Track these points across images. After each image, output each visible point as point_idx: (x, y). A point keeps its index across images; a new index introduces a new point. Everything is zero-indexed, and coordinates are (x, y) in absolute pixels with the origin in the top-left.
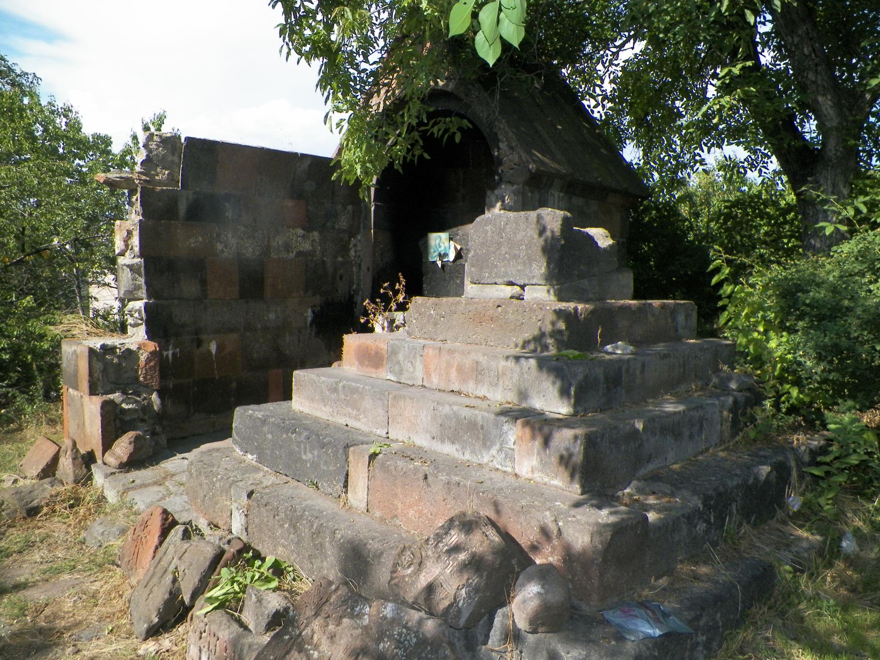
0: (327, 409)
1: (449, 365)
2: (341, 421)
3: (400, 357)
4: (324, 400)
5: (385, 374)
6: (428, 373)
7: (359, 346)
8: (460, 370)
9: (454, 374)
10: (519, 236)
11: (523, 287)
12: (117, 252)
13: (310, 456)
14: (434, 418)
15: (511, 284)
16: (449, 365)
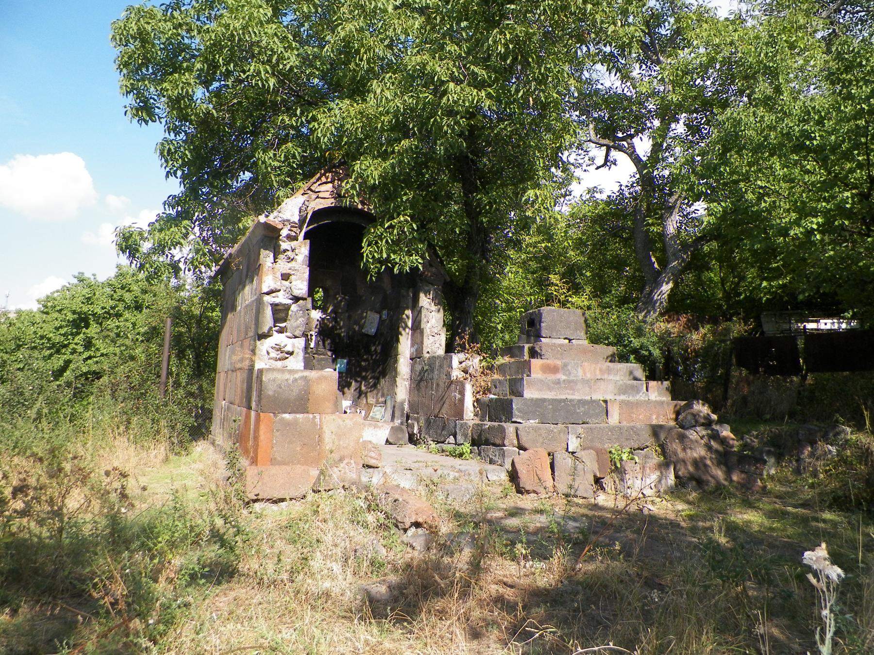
0: (553, 393)
1: (595, 369)
2: (564, 397)
3: (569, 367)
4: (550, 389)
5: (562, 377)
6: (585, 373)
7: (542, 365)
8: (601, 370)
9: (598, 372)
10: (571, 318)
11: (570, 340)
12: (265, 289)
13: (583, 409)
14: (615, 387)
15: (565, 339)
16: (595, 369)
